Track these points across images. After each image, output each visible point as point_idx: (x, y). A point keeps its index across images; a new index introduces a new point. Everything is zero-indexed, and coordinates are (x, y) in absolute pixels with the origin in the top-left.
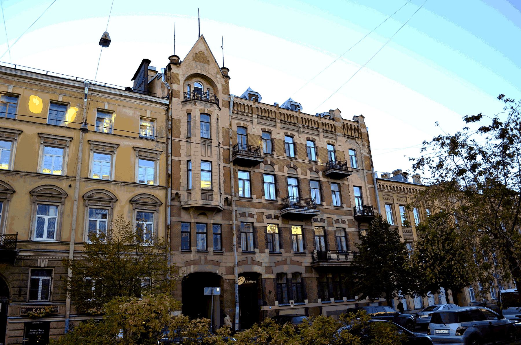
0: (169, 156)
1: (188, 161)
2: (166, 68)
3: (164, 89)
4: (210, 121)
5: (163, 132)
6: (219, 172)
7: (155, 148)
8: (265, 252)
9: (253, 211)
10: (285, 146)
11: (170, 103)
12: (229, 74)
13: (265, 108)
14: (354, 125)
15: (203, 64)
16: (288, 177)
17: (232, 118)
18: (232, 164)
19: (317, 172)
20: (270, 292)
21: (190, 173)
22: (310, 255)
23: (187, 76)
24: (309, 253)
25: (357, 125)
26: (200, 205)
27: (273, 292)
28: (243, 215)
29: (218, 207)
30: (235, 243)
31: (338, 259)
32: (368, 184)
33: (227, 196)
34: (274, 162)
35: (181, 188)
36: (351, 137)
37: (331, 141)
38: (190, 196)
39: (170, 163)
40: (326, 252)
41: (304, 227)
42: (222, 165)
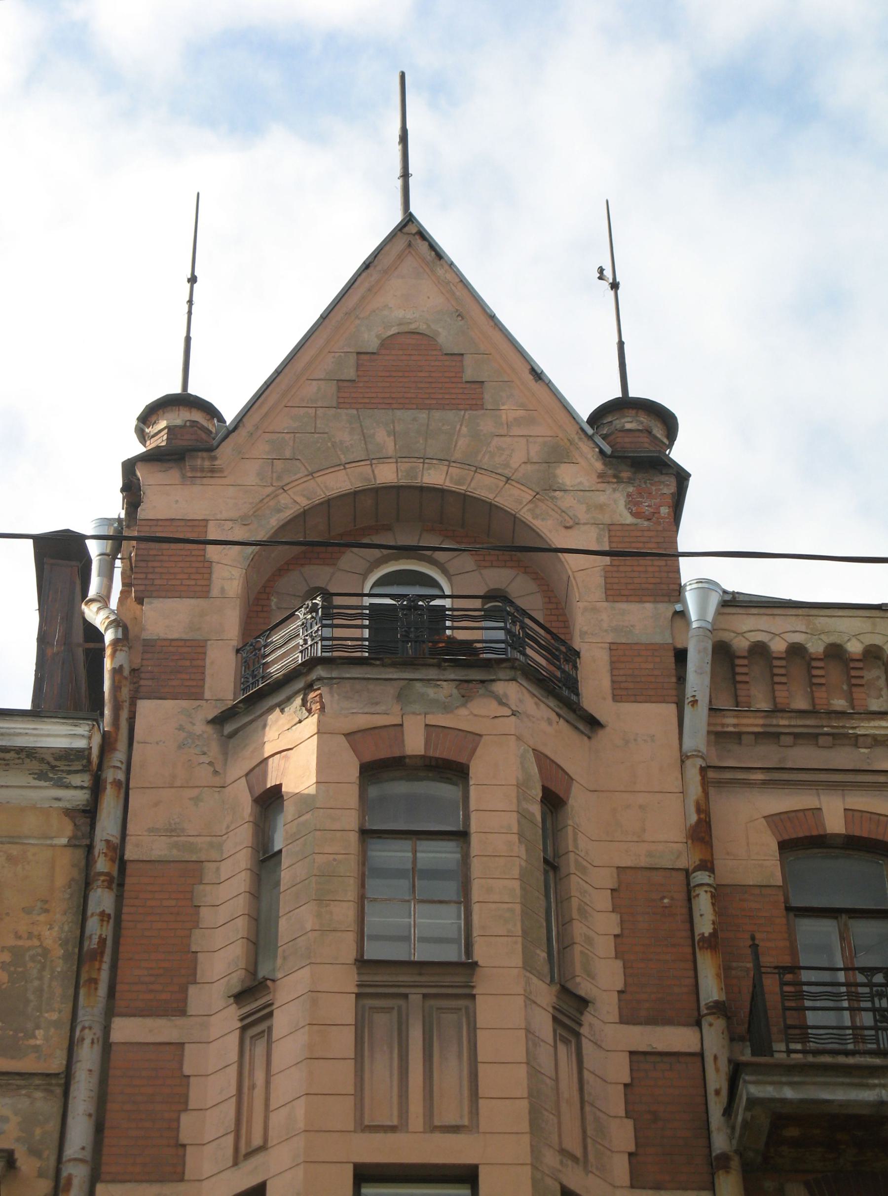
5: (40, 991)
15: (423, 415)
17: (705, 783)
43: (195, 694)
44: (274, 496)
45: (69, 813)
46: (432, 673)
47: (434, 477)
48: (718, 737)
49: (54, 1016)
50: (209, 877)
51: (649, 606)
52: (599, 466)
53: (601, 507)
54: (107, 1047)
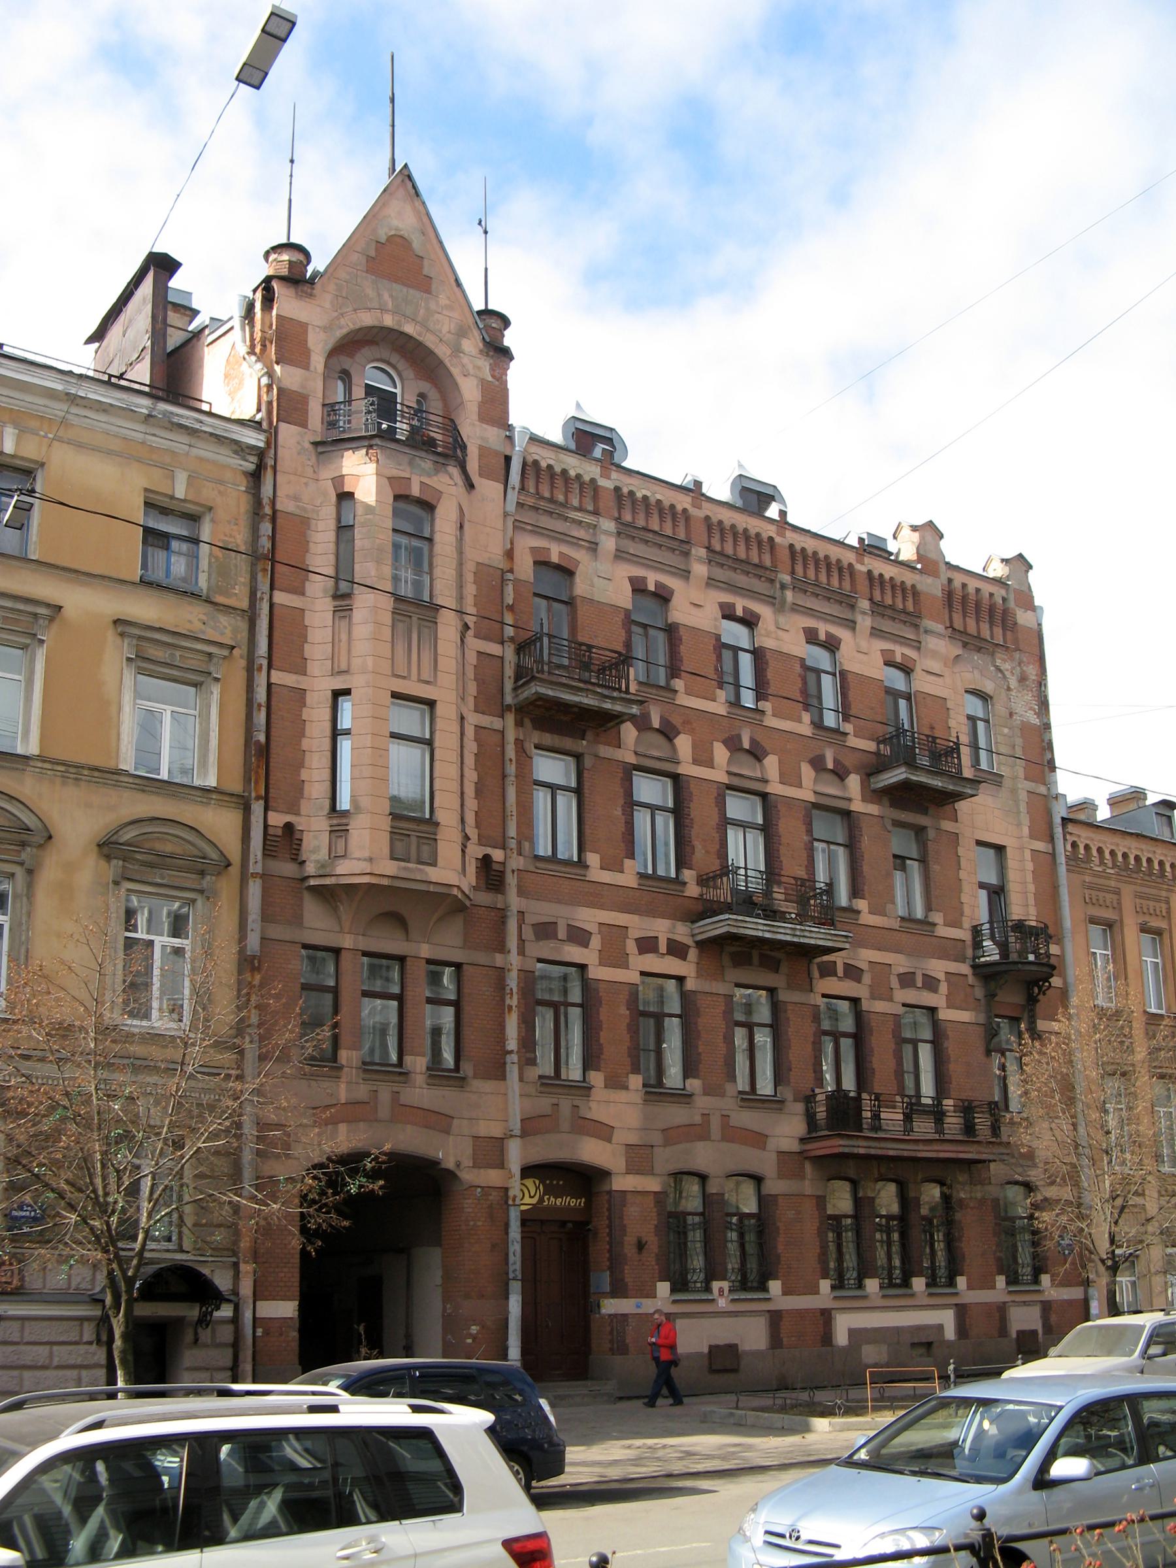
0: (260, 669)
1: (337, 694)
2: (251, 295)
3: (241, 383)
4: (432, 532)
5: (236, 566)
6: (462, 747)
7: (203, 632)
8: (626, 1088)
9: (589, 918)
10: (719, 658)
11: (268, 443)
12: (510, 339)
13: (649, 494)
14: (991, 595)
15: (405, 290)
16: (730, 787)
18: (510, 718)
19: (840, 774)
20: (641, 1246)
21: (345, 746)
22: (800, 1107)
23: (339, 333)
24: (795, 1100)
25: (1003, 592)
26: (385, 882)
27: (653, 1243)
28: (545, 931)
29: (455, 892)
30: (512, 1044)
31: (908, 1129)
32: (1033, 836)
33: (489, 851)
34: (676, 721)
35: (305, 807)
36: (972, 643)
37: (900, 652)
38: (341, 843)
39: (261, 695)
40: (858, 1099)
41: (783, 996)
42: (473, 719)
43: (303, 424)
44: (338, 318)
45: (246, 473)
46: (423, 454)
47: (409, 329)
48: (520, 505)
49: (242, 580)
50: (313, 527)
51: (495, 429)
52: (481, 345)
53: (479, 368)
54: (272, 605)
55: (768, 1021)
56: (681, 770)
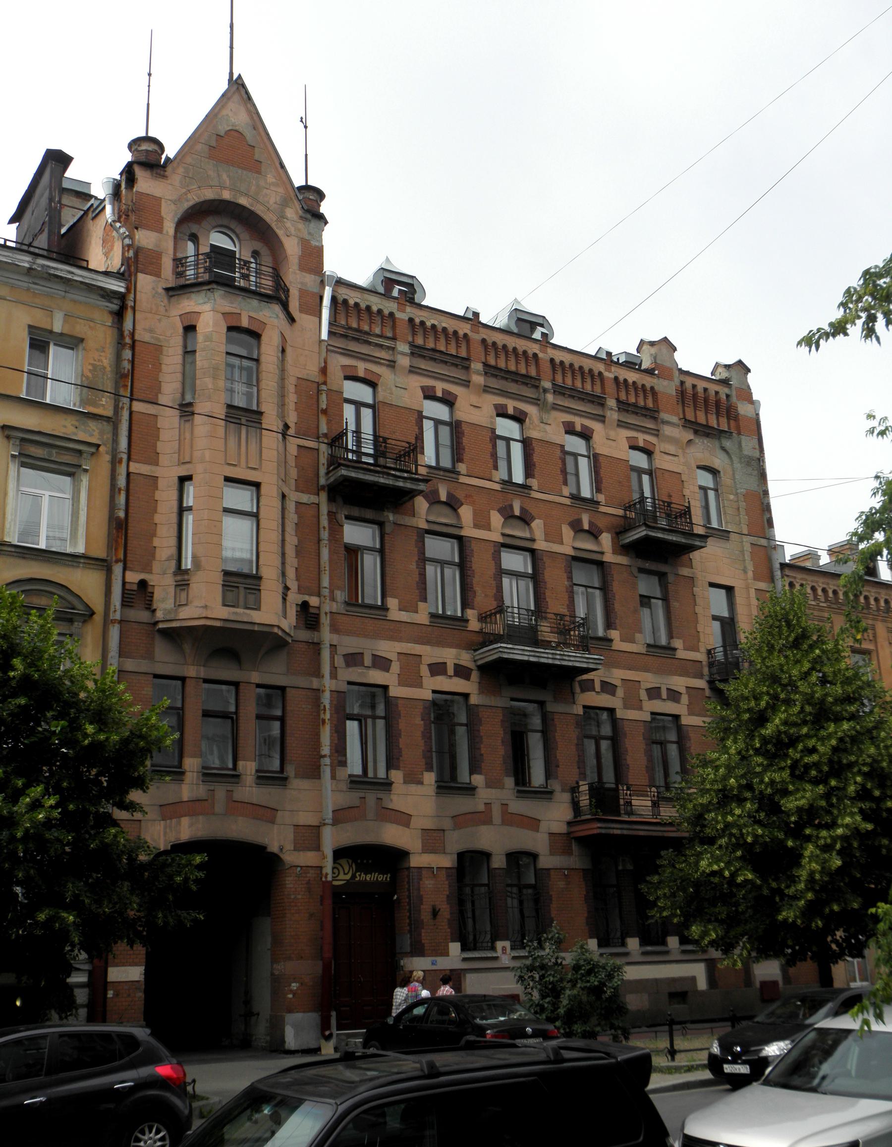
0: (120, 461)
1: (183, 480)
2: (118, 177)
3: (112, 246)
4: (259, 354)
6: (283, 518)
7: (75, 434)
8: (422, 783)
9: (388, 648)
10: (494, 446)
11: (128, 289)
12: (325, 208)
13: (436, 323)
14: (717, 393)
15: (240, 171)
16: (504, 545)
17: (327, 350)
18: (324, 496)
19: (594, 534)
20: (435, 913)
21: (189, 520)
22: (567, 797)
23: (186, 205)
24: (563, 791)
25: (727, 390)
26: (218, 624)
27: (446, 911)
28: (354, 659)
29: (276, 630)
30: (326, 750)
31: (656, 814)
32: (756, 578)
33: (306, 598)
34: (460, 494)
35: (156, 567)
36: (703, 431)
37: (642, 439)
38: (183, 595)
39: (122, 482)
40: (616, 790)
41: (550, 707)
42: (294, 496)
43: (158, 275)
47: (243, 201)
50: (164, 353)
53: (299, 230)
54: (131, 413)
55: (540, 728)
56: (463, 533)
